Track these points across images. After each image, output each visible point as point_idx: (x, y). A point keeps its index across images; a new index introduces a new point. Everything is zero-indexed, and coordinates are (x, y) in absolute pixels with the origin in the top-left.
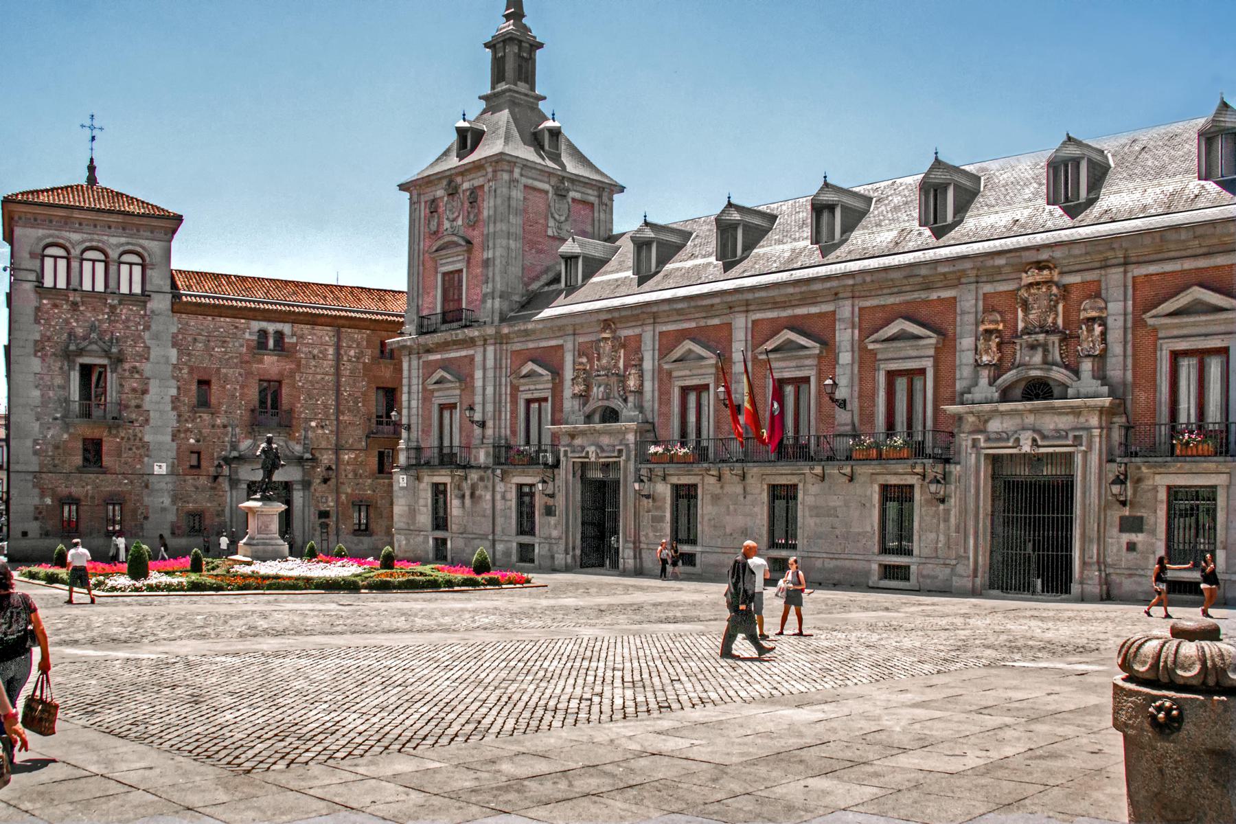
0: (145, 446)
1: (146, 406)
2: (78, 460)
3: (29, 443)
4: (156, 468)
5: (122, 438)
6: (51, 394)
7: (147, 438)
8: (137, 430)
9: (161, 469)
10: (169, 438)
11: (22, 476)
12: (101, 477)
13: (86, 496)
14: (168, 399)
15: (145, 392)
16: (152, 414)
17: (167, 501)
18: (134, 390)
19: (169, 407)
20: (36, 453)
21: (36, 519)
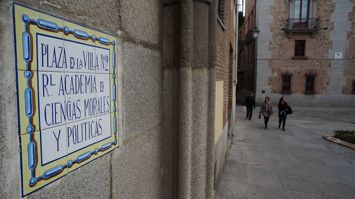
0: (331, 43)
1: (332, 20)
2: (291, 52)
3: (267, 44)
4: (336, 55)
5: (317, 39)
6: (279, 17)
7: (331, 39)
8: (326, 34)
9: (339, 55)
10: (346, 37)
11: (263, 61)
12: (304, 61)
13: (296, 72)
14: (347, 15)
15: (332, 11)
16: (335, 25)
17: (341, 74)
18: (326, 11)
19: (346, 19)
20: (270, 49)
21: (269, 84)
